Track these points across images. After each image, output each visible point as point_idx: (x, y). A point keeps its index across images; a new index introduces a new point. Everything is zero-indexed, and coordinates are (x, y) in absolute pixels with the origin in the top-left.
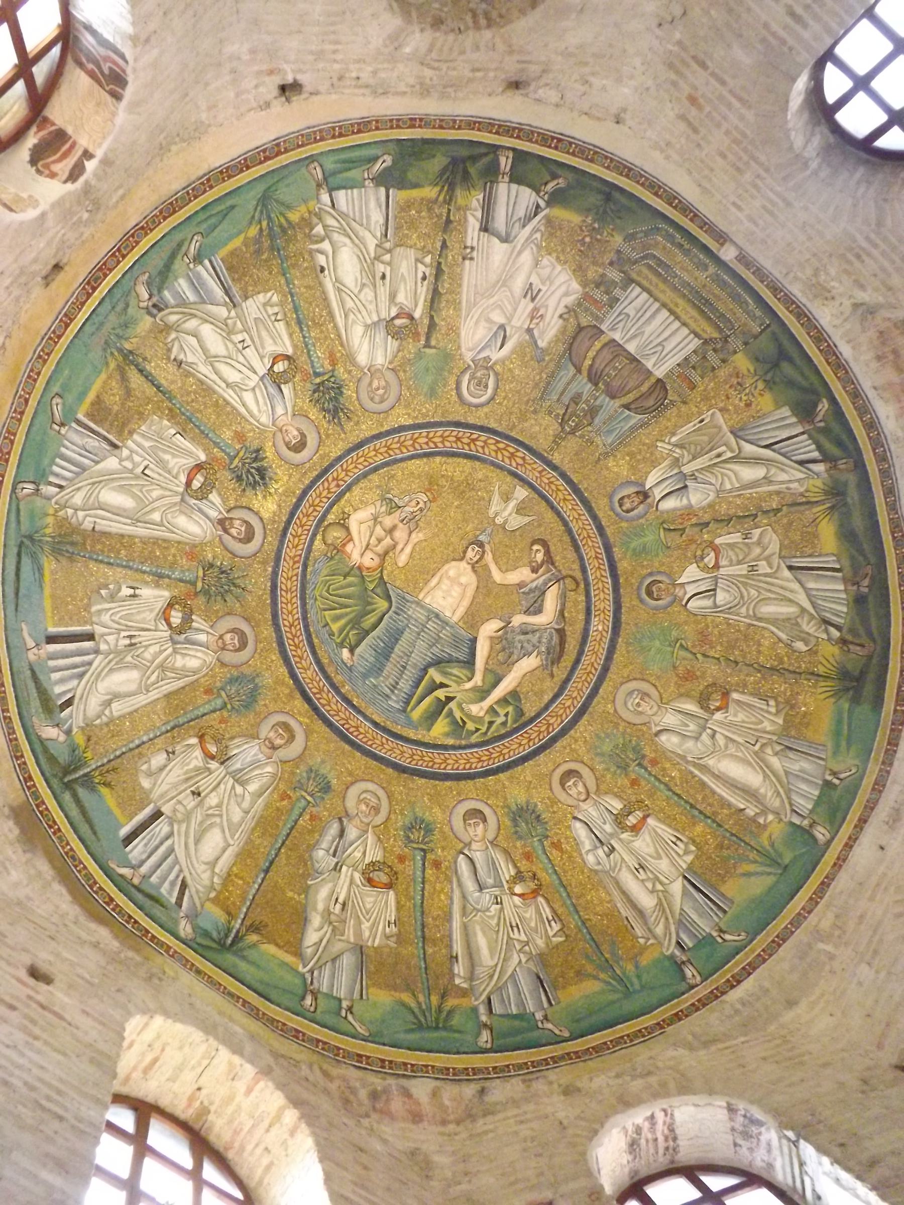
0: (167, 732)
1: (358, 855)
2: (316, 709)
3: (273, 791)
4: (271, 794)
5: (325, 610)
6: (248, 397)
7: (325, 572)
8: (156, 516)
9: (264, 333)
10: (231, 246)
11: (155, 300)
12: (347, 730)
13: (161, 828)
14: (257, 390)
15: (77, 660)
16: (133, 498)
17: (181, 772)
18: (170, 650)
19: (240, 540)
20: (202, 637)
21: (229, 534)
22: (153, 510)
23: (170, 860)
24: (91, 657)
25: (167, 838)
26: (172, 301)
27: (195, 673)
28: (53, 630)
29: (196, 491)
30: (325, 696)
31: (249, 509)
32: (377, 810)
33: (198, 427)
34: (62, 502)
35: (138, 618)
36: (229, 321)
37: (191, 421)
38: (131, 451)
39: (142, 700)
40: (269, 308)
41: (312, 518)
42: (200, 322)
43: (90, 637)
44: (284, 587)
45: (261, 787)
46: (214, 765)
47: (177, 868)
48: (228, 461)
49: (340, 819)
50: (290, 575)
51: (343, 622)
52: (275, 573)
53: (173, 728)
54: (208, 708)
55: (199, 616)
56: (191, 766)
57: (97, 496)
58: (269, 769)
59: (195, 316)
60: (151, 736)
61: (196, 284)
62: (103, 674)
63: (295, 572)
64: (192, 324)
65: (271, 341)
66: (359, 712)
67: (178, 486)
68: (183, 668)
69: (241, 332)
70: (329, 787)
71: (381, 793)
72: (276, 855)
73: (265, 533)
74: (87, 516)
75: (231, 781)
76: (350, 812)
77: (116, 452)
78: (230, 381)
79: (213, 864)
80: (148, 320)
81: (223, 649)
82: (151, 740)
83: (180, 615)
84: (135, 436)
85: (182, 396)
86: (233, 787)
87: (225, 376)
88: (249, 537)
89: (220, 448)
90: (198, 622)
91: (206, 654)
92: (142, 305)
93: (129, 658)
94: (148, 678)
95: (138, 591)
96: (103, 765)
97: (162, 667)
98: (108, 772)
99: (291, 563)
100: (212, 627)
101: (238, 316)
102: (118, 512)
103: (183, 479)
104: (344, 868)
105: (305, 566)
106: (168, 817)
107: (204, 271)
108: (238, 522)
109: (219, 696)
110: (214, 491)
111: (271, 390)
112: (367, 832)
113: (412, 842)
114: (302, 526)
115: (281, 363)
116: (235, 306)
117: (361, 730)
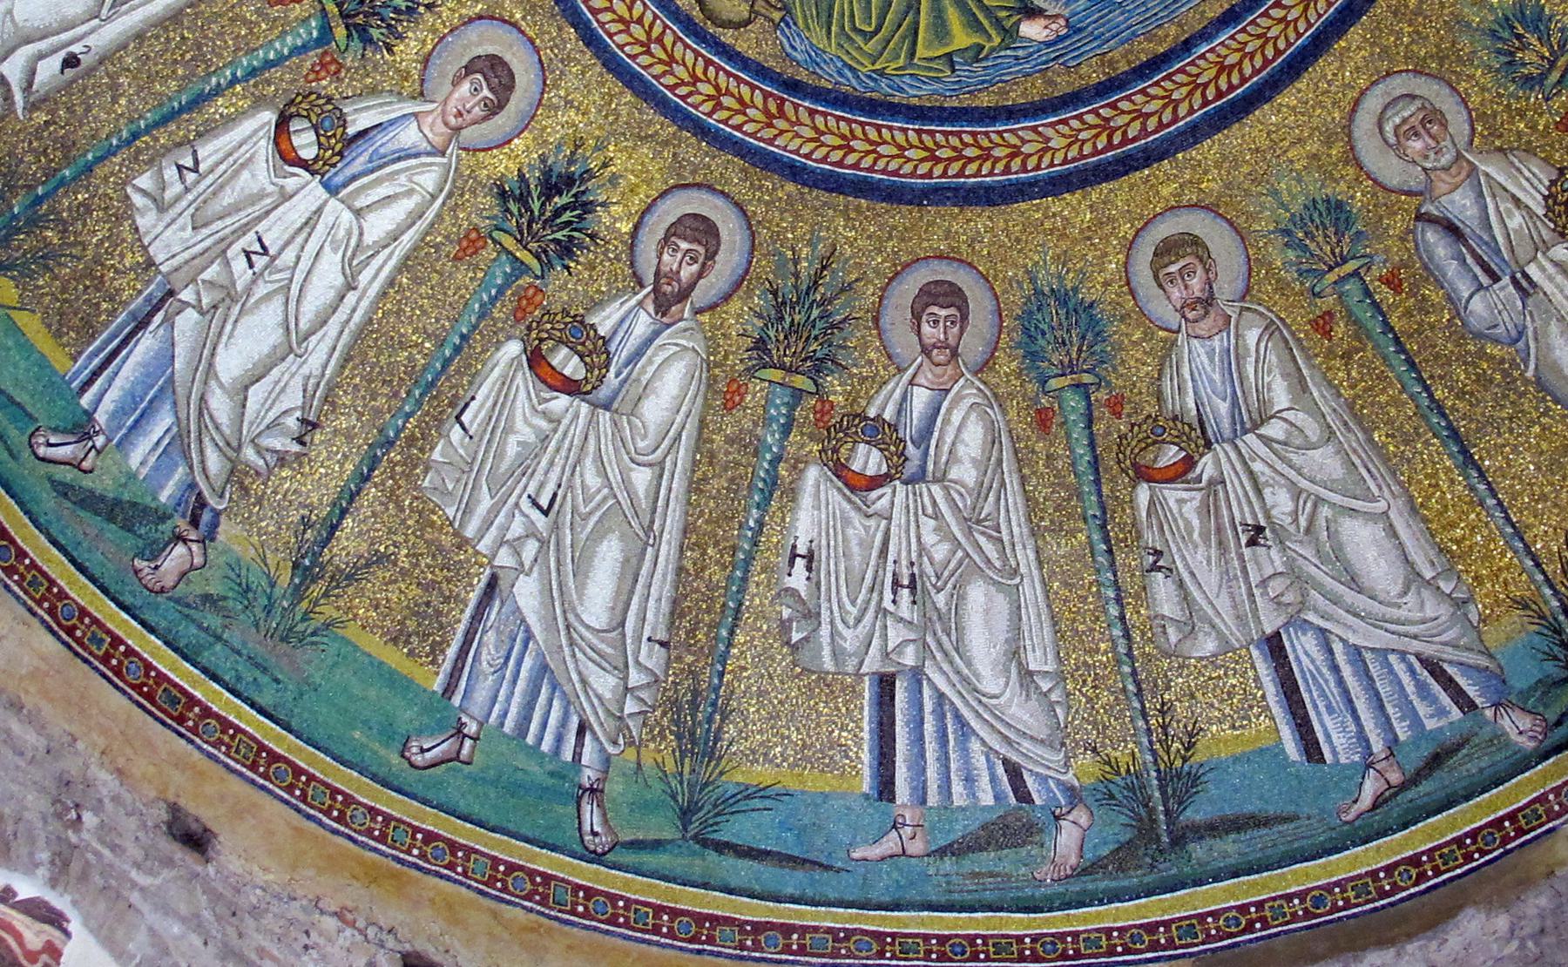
0: (1110, 552)
1: (1516, 221)
2: (1149, 157)
3: (1302, 349)
4: (1308, 358)
5: (912, 54)
6: (378, 225)
7: (818, 37)
8: (642, 478)
9: (227, 198)
10: (43, 341)
11: (182, 524)
12: (1220, 94)
13: (1303, 650)
14: (358, 204)
15: (929, 727)
16: (602, 538)
17: (1201, 550)
18: (936, 490)
19: (711, 256)
20: (921, 398)
21: (692, 286)
22: (627, 483)
23: (1374, 670)
24: (927, 692)
25: (1331, 652)
26: (180, 472)
27: (993, 441)
28: (866, 784)
29: (590, 368)
30: (1121, 121)
31: (636, 227)
32: (1433, 116)
33: (447, 362)
34: (611, 724)
35: (857, 559)
36: (205, 301)
37: (432, 384)
38: (502, 542)
39: (1031, 592)
40: (169, 194)
41: (678, 51)
42: (213, 383)
43: (885, 685)
44: (836, 156)
45: (1285, 376)
46: (1206, 467)
47: (1392, 658)
48: (526, 280)
49: (1419, 217)
50: (812, 134)
51: (953, 17)
52: (794, 172)
53: (1106, 540)
54: (1078, 432)
55: (870, 399)
56: (1196, 523)
57: (597, 631)
58: (1252, 336)
59: (202, 398)
60: (1111, 594)
61: (137, 414)
62: (966, 671)
63: (804, 116)
64: (220, 405)
65: (245, 174)
66: (1187, 46)
67: (576, 416)
68: (982, 465)
69: (227, 264)
70: (1340, 205)
71: (1398, 85)
72: (1444, 416)
73: (699, 186)
74: (637, 663)
75: (1250, 438)
76: (1413, 185)
77: (503, 584)
78: (340, 280)
79: (1413, 577)
80: (226, 530)
81: (955, 354)
82: (1119, 600)
83: (862, 448)
84: (470, 532)
85: (378, 412)
86: (1267, 441)
87: (332, 294)
88: (703, 231)
89: (493, 300)
90: (883, 406)
91: (959, 398)
92: (198, 560)
93: (941, 599)
94: (988, 561)
95: (801, 550)
96: (1149, 731)
97: (971, 522)
98: (1164, 727)
99: (781, 124)
100: (901, 370)
101: (194, 280)
102: (630, 574)
103: (561, 402)
104: (1532, 270)
105: (793, 87)
106: (1286, 625)
107: (106, 401)
108: (666, 257)
109: (1058, 394)
110: (593, 319)
111: (357, 166)
112: (1473, 168)
113: (1543, 76)
114: (696, 79)
115: (296, 141)
116: (171, 293)
117: (1233, 58)
